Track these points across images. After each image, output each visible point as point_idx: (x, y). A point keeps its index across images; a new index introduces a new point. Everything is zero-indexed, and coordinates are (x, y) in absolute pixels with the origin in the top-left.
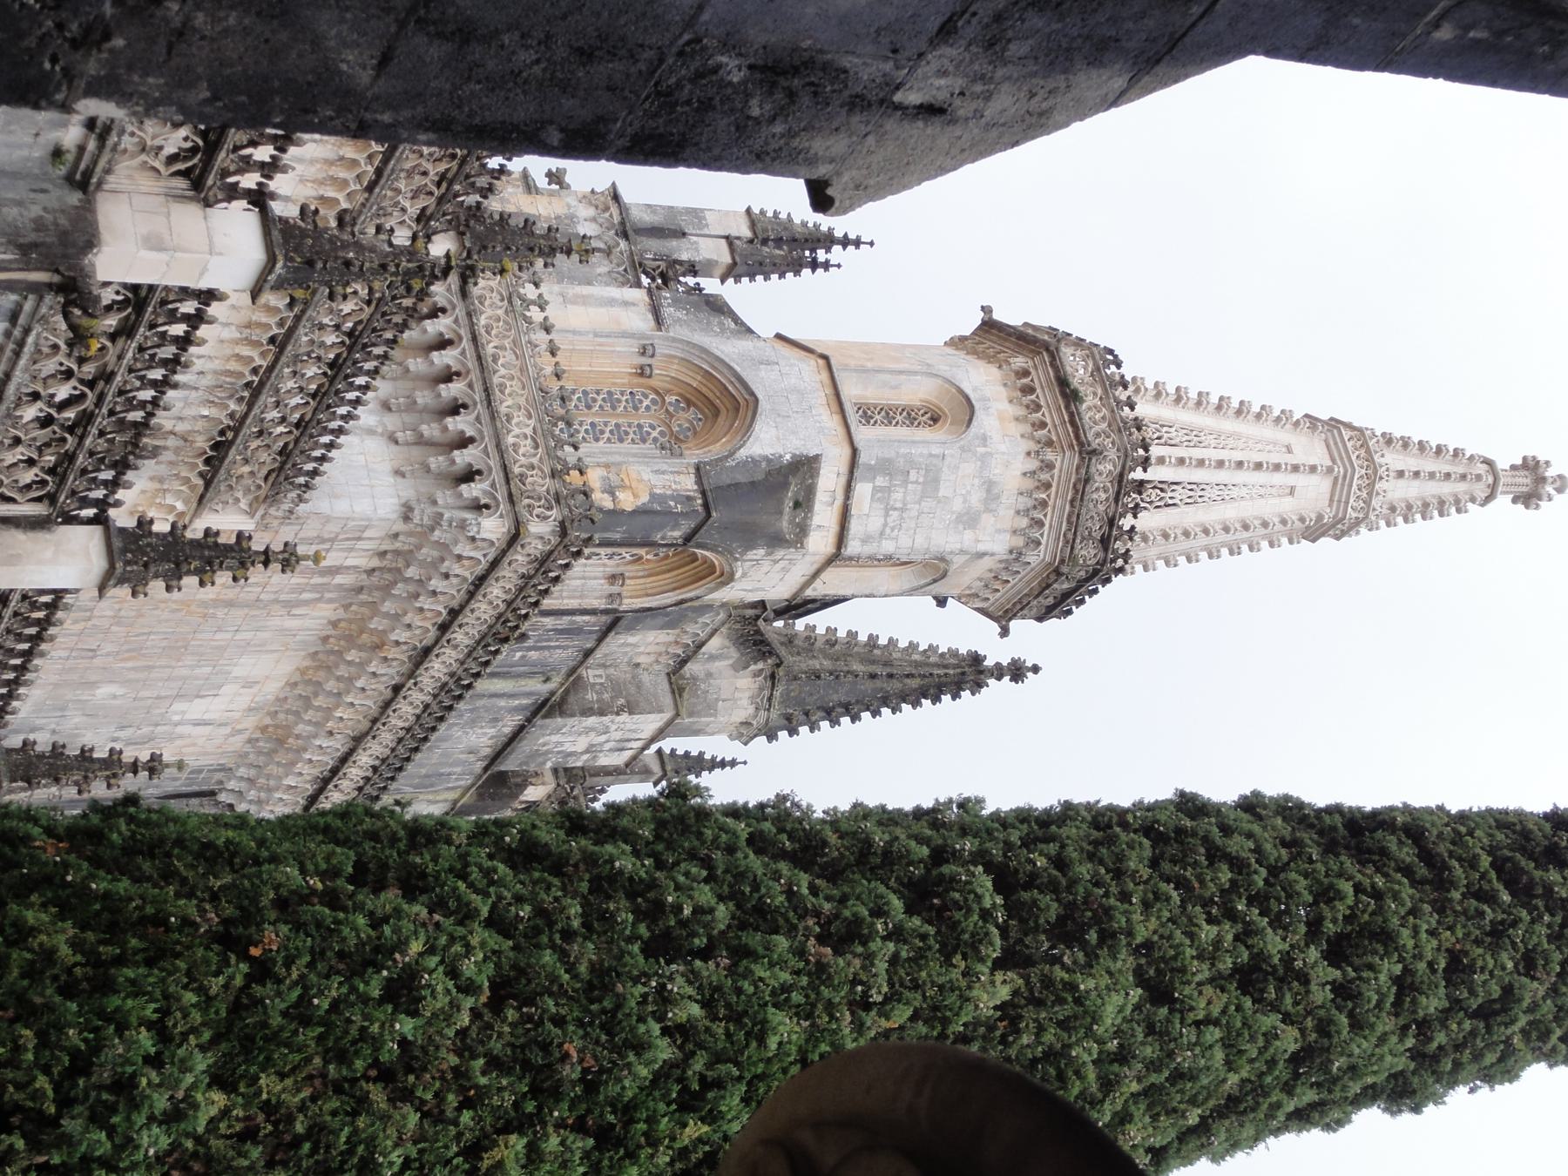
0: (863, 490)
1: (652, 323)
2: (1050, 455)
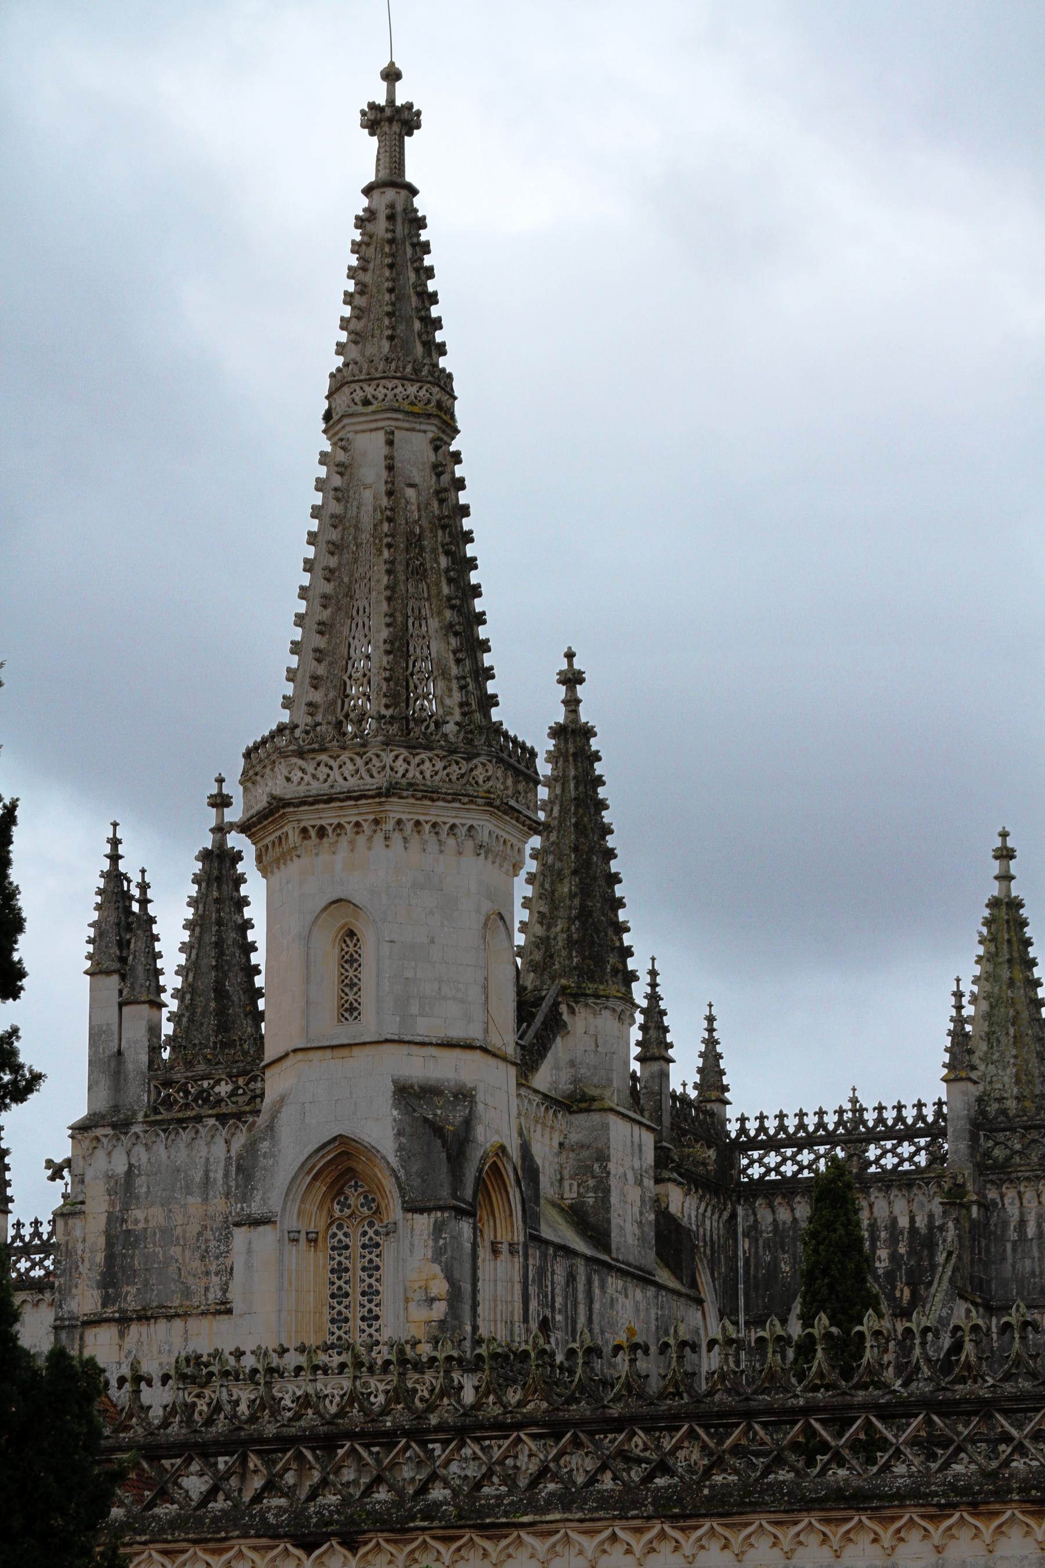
0: (425, 1027)
1: (267, 1228)
2: (390, 825)
